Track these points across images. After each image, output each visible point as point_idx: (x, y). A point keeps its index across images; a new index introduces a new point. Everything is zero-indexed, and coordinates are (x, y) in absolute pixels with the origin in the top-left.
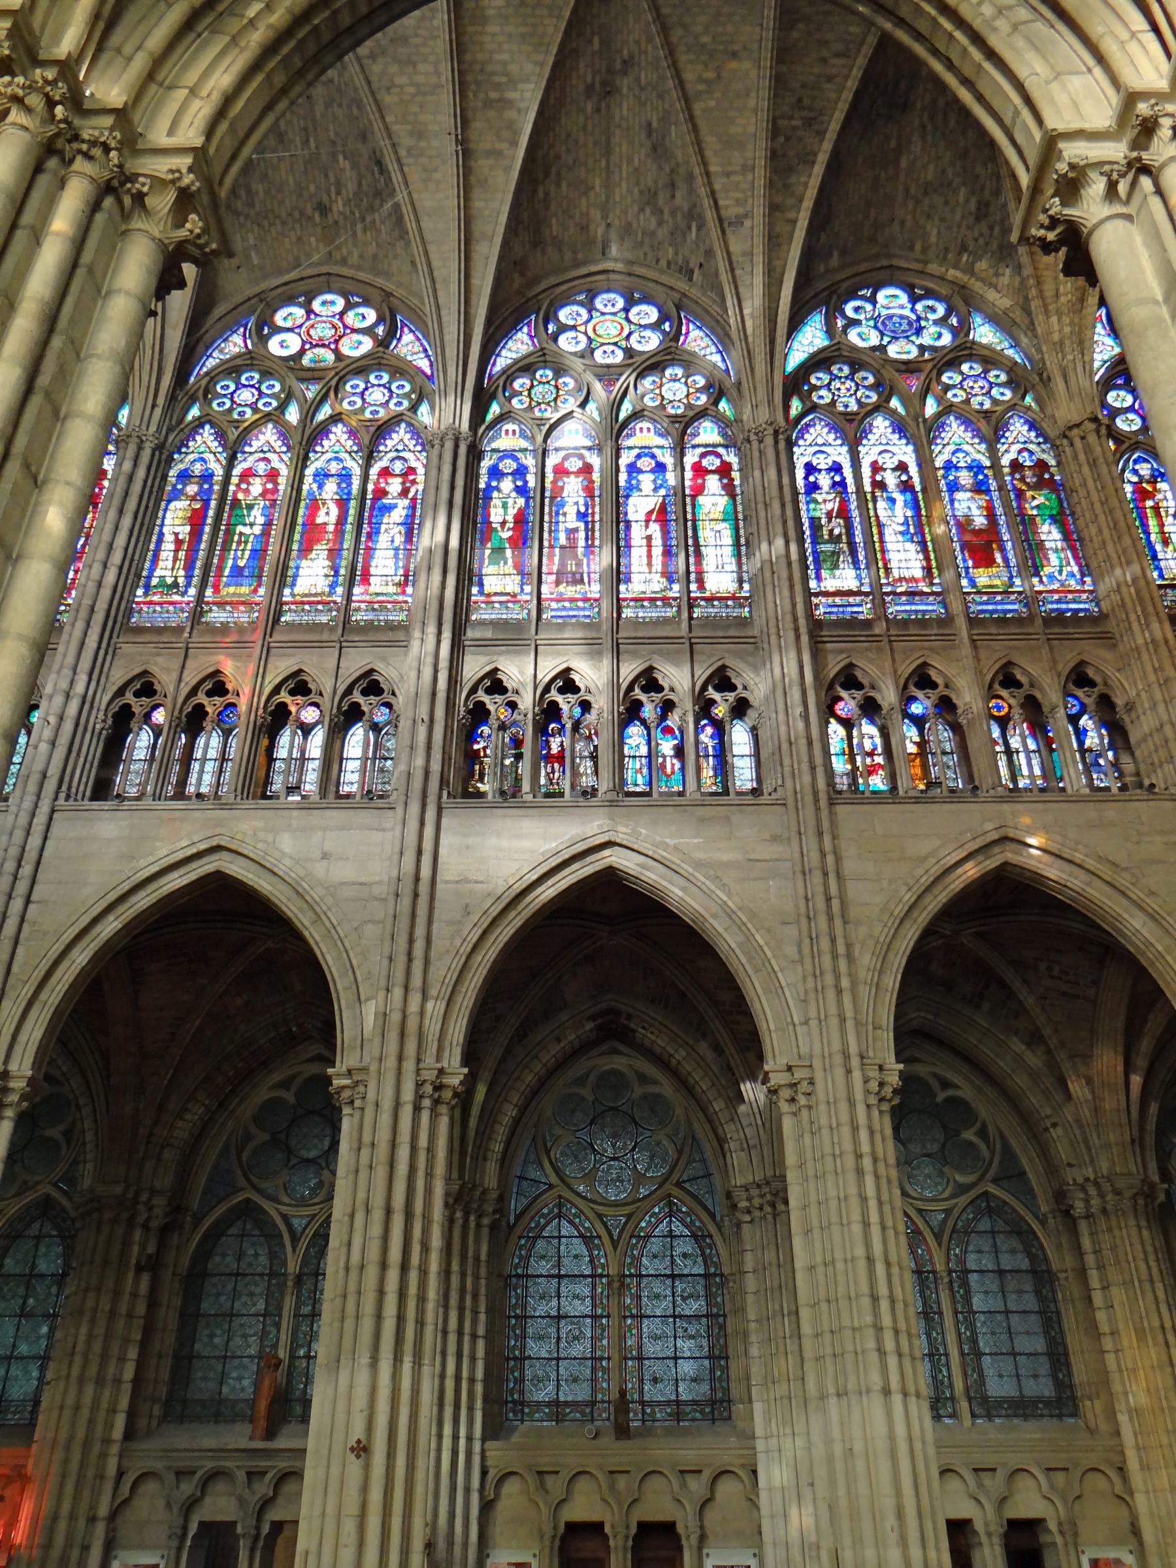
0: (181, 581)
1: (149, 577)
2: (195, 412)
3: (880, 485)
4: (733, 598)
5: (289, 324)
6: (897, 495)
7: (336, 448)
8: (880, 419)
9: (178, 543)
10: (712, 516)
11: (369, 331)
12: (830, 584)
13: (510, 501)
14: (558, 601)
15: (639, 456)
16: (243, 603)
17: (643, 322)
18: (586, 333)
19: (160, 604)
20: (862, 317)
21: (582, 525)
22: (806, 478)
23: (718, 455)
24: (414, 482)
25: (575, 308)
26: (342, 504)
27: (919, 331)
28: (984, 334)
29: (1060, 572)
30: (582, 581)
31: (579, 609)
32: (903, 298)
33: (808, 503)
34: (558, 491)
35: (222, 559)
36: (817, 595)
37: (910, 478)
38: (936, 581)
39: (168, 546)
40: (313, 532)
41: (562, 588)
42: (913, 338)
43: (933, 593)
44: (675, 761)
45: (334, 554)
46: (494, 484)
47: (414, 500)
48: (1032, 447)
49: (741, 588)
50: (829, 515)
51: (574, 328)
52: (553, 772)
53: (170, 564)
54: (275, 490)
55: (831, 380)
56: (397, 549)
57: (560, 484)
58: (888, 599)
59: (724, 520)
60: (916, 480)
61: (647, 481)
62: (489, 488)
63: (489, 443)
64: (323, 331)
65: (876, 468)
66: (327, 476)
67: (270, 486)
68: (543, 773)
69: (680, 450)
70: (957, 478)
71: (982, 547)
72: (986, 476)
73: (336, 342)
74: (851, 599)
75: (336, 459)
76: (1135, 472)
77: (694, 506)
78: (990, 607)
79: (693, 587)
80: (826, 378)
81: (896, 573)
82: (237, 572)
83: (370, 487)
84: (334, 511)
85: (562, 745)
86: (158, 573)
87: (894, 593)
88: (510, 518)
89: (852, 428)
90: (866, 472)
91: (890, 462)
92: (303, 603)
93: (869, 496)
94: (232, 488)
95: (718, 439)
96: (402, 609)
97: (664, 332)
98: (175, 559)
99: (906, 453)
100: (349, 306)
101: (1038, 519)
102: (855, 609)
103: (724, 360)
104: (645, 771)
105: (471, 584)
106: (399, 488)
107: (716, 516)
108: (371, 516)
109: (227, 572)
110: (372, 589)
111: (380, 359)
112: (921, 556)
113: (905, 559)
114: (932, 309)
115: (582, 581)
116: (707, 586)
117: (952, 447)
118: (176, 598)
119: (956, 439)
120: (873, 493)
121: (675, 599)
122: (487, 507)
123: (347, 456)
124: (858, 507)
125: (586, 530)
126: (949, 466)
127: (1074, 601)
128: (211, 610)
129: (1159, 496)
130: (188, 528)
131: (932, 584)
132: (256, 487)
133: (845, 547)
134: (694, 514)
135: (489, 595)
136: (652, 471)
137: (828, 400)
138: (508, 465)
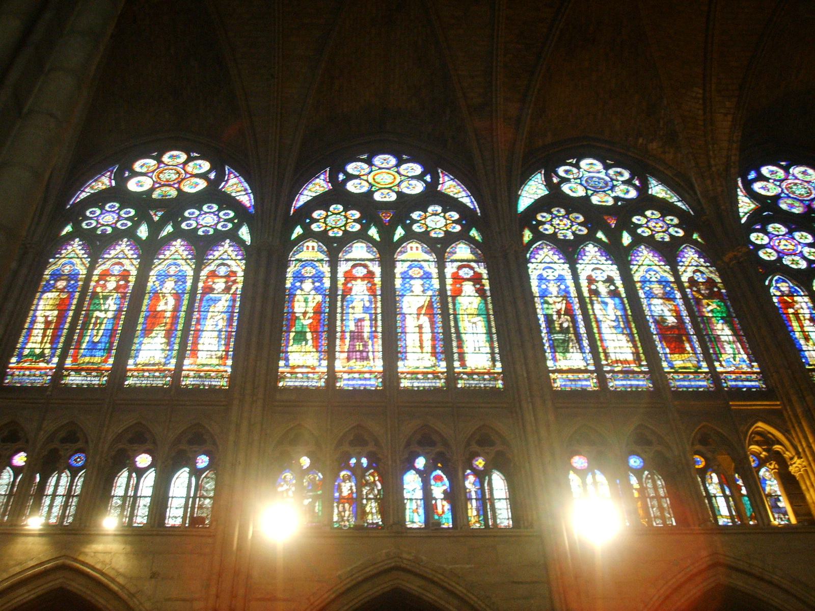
0: (47, 352)
1: (23, 348)
3: (596, 293)
4: (489, 373)
5: (144, 170)
6: (608, 300)
8: (591, 246)
9: (47, 323)
10: (469, 312)
11: (203, 176)
12: (563, 364)
13: (310, 298)
14: (349, 373)
15: (410, 267)
16: (94, 370)
17: (410, 175)
18: (367, 181)
19: (29, 369)
20: (571, 177)
21: (367, 316)
22: (539, 286)
23: (472, 268)
25: (359, 164)
26: (178, 297)
27: (613, 188)
29: (734, 358)
30: (367, 358)
31: (365, 379)
32: (599, 166)
34: (347, 292)
35: (82, 336)
36: (554, 372)
37: (617, 288)
39: (39, 325)
40: (155, 317)
41: (352, 363)
42: (609, 192)
43: (642, 372)
44: (445, 503)
45: (169, 334)
46: (298, 284)
47: (235, 294)
48: (702, 269)
49: (494, 366)
50: (558, 312)
51: (358, 177)
52: (344, 511)
53: (39, 339)
54: (126, 286)
55: (552, 218)
57: (349, 285)
58: (609, 376)
59: (478, 315)
60: (622, 290)
61: (417, 285)
62: (294, 287)
63: (294, 255)
65: (591, 280)
67: (122, 283)
68: (336, 511)
69: (441, 264)
71: (675, 338)
72: (672, 288)
73: (179, 183)
74: (581, 376)
75: (175, 264)
76: (778, 289)
77: (454, 304)
78: (686, 383)
79: (457, 364)
80: (549, 217)
81: (613, 357)
82: (93, 346)
83: (201, 285)
84: (171, 302)
85: (351, 489)
86: (29, 345)
88: (310, 310)
90: (584, 283)
91: (600, 276)
92: (144, 370)
93: (588, 300)
94: (93, 284)
95: (471, 257)
96: (222, 377)
97: (425, 181)
98: (44, 336)
99: (613, 270)
100: (190, 159)
101: (713, 319)
103: (472, 202)
104: (421, 511)
105: (279, 359)
106: (223, 286)
107: (472, 312)
108: (200, 307)
109: (84, 346)
110: (199, 361)
111: (213, 194)
112: (630, 345)
113: (619, 347)
114: (621, 174)
115: (367, 358)
116: (468, 363)
117: (645, 268)
118: (42, 365)
119: (647, 262)
120: (590, 298)
121: (442, 373)
122: (292, 301)
123: (183, 262)
125: (371, 320)
126: (644, 281)
127: (747, 380)
128: (69, 375)
129: (797, 306)
131: (641, 366)
132: (111, 284)
133: (573, 337)
134: (454, 309)
135: (293, 367)
136: (421, 278)
138: (309, 271)
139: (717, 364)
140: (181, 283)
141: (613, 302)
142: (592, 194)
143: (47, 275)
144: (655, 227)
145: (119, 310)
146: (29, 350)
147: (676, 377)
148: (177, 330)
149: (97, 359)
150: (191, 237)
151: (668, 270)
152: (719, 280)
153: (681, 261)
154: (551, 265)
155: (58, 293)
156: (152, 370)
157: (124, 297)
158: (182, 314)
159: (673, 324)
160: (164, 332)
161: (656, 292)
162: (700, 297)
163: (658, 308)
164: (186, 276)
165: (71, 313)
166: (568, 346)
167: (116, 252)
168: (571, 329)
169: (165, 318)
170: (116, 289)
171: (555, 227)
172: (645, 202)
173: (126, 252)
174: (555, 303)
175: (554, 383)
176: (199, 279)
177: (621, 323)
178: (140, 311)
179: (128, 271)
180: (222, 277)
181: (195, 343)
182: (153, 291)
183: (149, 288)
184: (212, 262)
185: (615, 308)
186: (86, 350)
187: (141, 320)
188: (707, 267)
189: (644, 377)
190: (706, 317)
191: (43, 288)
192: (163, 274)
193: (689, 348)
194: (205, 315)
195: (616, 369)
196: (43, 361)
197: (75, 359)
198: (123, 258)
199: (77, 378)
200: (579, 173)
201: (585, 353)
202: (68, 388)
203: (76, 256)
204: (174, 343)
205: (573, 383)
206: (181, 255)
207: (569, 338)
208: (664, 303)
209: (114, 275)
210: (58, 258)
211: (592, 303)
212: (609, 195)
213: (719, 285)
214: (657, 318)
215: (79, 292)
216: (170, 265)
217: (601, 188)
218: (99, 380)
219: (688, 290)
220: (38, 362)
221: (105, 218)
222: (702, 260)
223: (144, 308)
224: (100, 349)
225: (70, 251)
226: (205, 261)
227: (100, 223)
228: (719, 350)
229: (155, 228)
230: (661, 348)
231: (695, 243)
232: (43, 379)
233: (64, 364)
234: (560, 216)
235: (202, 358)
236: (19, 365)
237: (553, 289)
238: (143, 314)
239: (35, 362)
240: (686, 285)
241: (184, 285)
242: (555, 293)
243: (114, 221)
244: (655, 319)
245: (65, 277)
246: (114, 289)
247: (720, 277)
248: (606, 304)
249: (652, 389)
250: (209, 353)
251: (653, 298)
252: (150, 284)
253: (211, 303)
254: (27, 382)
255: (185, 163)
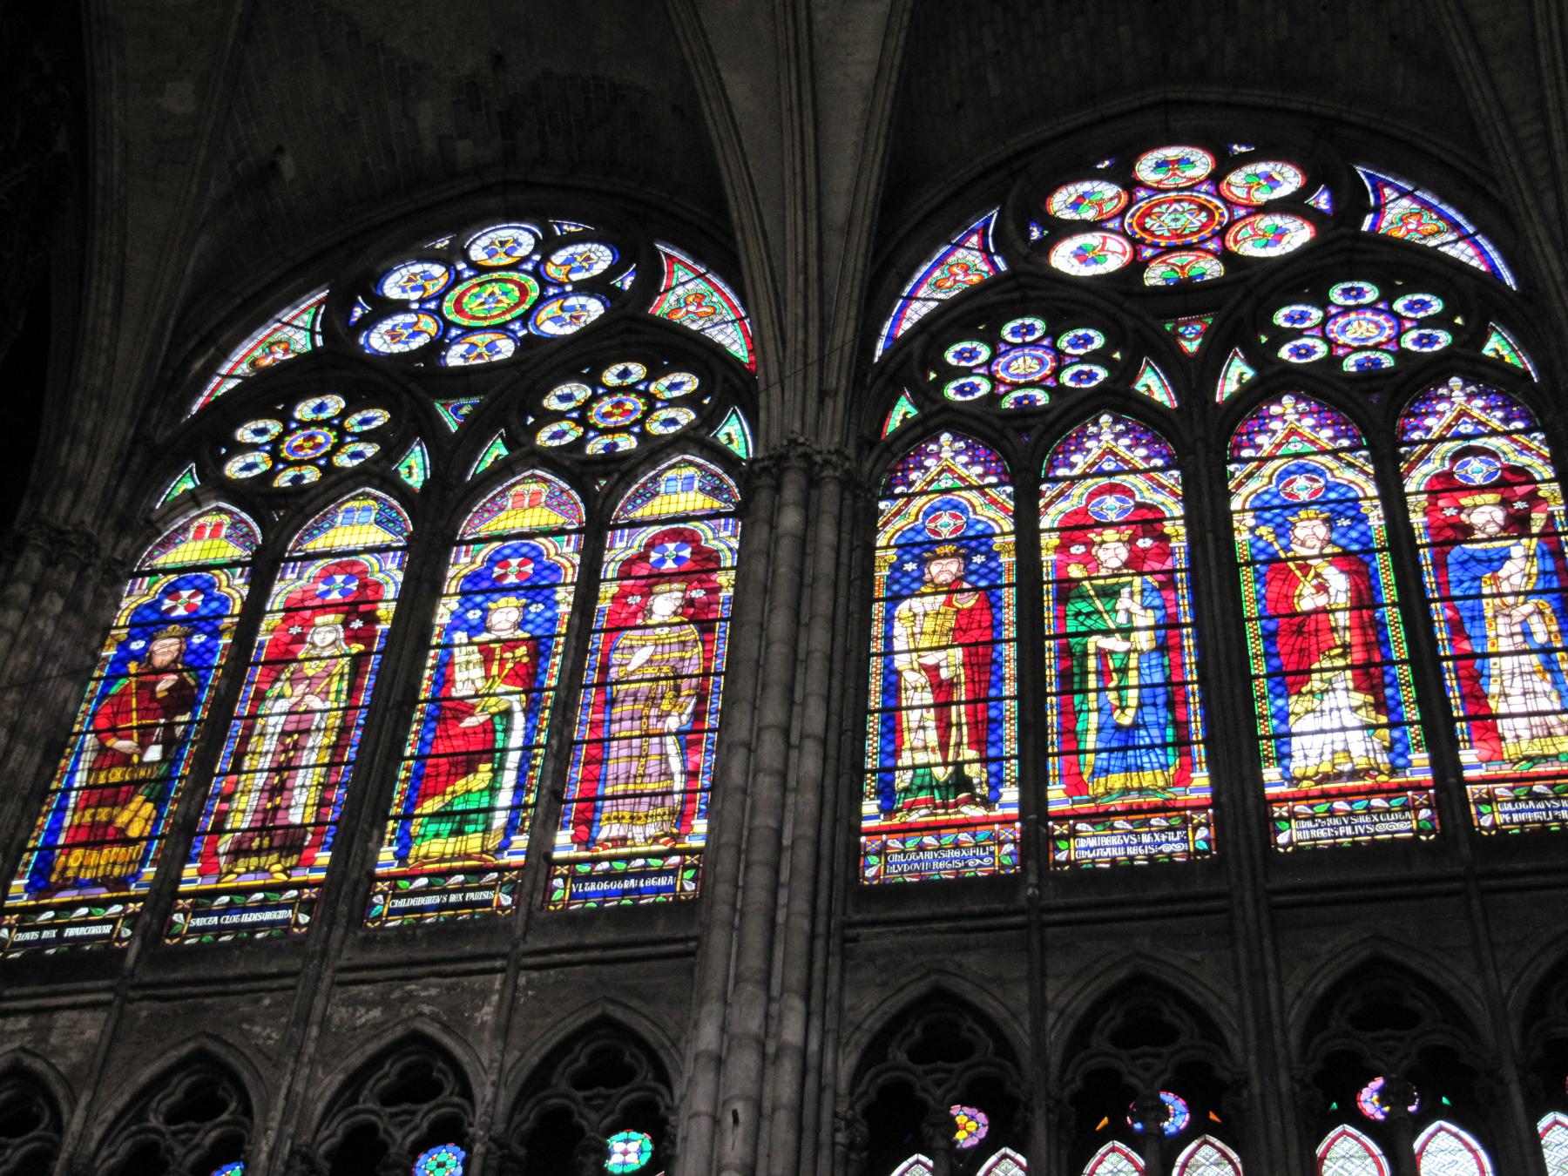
0: (972, 771)
1: (887, 771)
2: (903, 409)
7: (1295, 446)
9: (942, 690)
24: (1534, 499)
26: (1354, 561)
35: (1070, 715)
39: (916, 692)
45: (1371, 677)
53: (932, 737)
56: (1546, 651)
64: (1172, 220)
66: (1295, 507)
67: (1145, 543)
73: (1221, 234)
75: (1302, 470)
82: (1123, 741)
84: (1339, 582)
86: (906, 759)
92: (1326, 796)
94: (1048, 557)
98: (944, 727)
108: (1443, 585)
109: (1091, 742)
123: (1327, 460)
128: (1074, 834)
130: (957, 654)
140: (1348, 522)
143: (888, 547)
145: (1168, 626)
146: (910, 773)
148: (1393, 663)
149: (1147, 779)
150: (1325, 387)
155: (942, 598)
156: (1357, 792)
157: (1168, 583)
158: (1392, 615)
160: (1349, 673)
164: (1357, 499)
165: (1009, 651)
167: (1090, 458)
169: (1334, 630)
170: (1136, 562)
173: (1121, 451)
176: (1405, 503)
178: (1240, 621)
179: (1152, 508)
180: (1481, 489)
181: (1475, 696)
182: (1262, 557)
183: (1243, 553)
184: (1427, 451)
186: (1104, 755)
187: (1255, 646)
191: (888, 589)
192: (1276, 502)
194: (1472, 609)
196: (971, 800)
197: (1076, 786)
198: (1121, 472)
199: (1106, 841)
202: (1082, 876)
203: (959, 484)
204: (1400, 704)
206: (1313, 442)
209: (1111, 525)
210: (902, 495)
215: (1010, 585)
216: (1288, 473)
218: (1185, 840)
220: (956, 805)
221: (1014, 364)
223: (1250, 609)
224: (1152, 747)
225: (934, 471)
226: (1403, 450)
227: (1002, 382)
229: (1194, 377)
232: (992, 854)
233: (1044, 802)
235: (1518, 737)
236: (896, 821)
238: (1253, 630)
239: (945, 806)
241: (1362, 527)
243: (1047, 371)
245: (949, 549)
246: (1126, 565)
250: (1536, 720)
252: (1242, 537)
253: (1477, 570)
254: (942, 868)
255: (1216, 178)
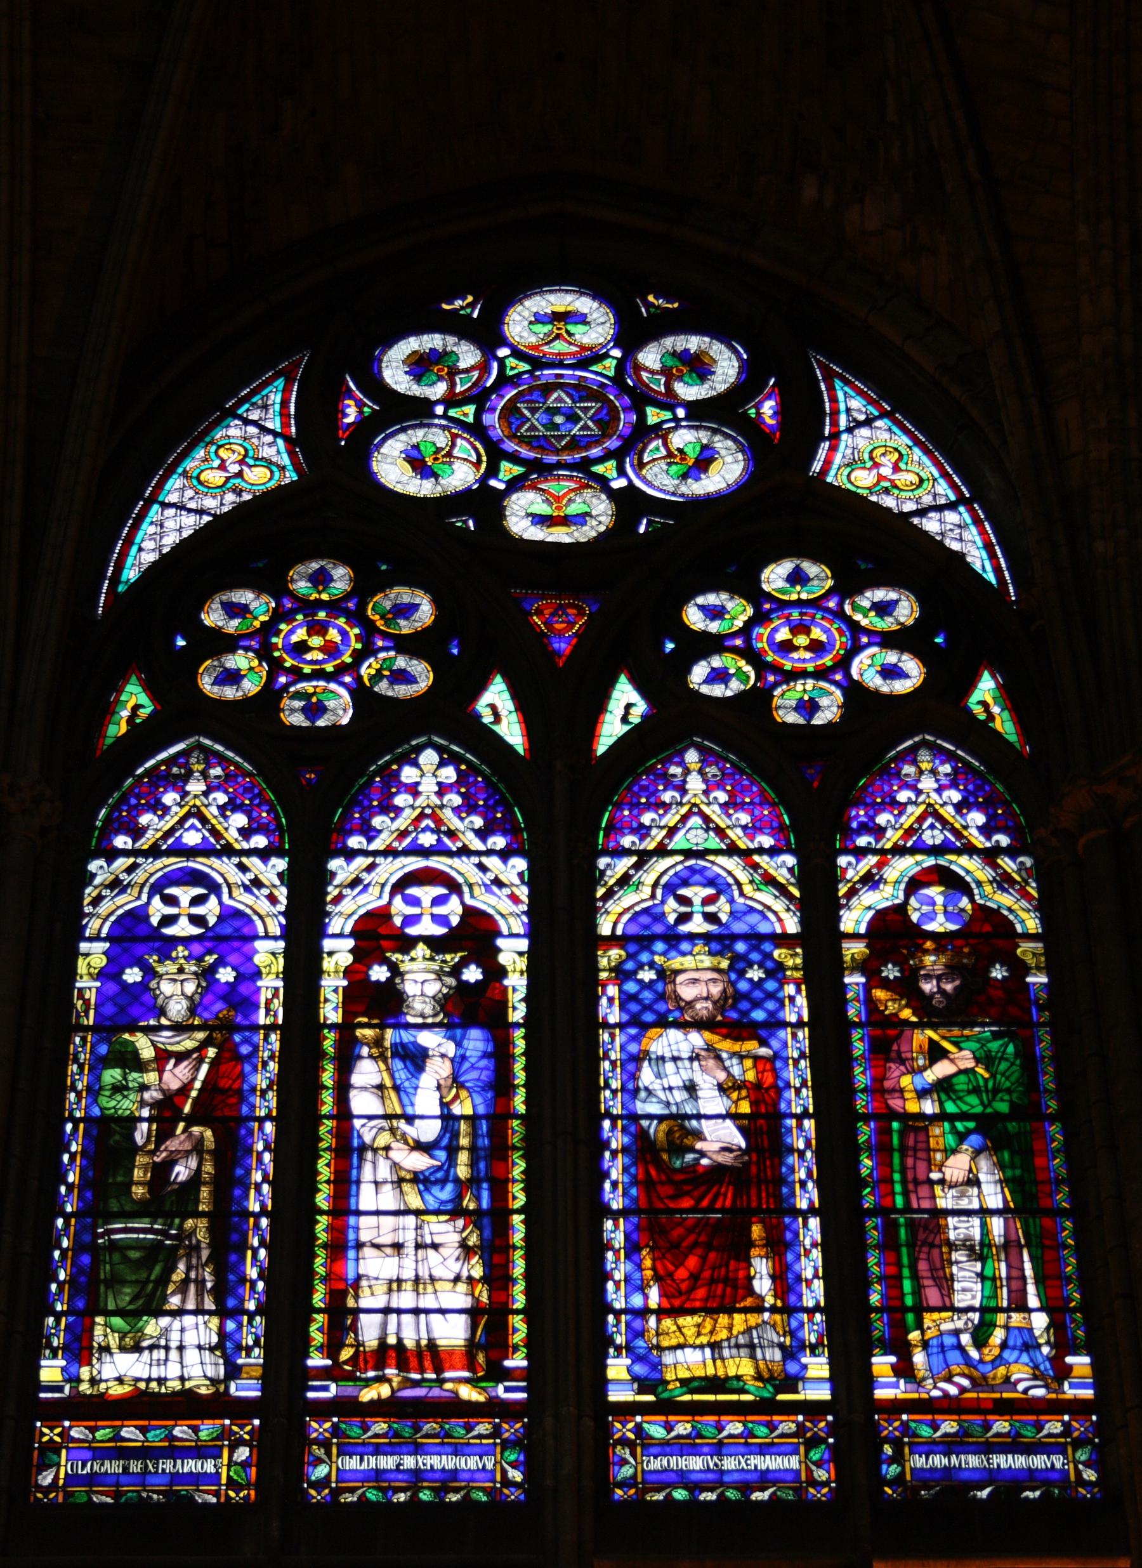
3: (379, 1003)
12: (119, 1370)
22: (109, 974)
28: (875, 457)
29: (980, 1338)
33: (99, 1064)
36: (57, 1411)
38: (517, 1361)
43: (493, 1408)
48: (967, 865)
50: (167, 1111)
55: (279, 615)
60: (516, 983)
70: (666, 975)
71: (708, 1225)
72: (776, 971)
78: (696, 1463)
81: (369, 1330)
87: (347, 1407)
89: (315, 794)
90: (338, 954)
91: (428, 914)
99: (499, 886)
102: (190, 1466)
113: (414, 1273)
114: (699, 366)
119: (693, 836)
120: (345, 1030)
124: (281, 1083)
127: (1014, 1445)
131: (497, 1373)
133: (200, 1228)
137: (251, 686)
139: (882, 1363)
141: (450, 1049)
142: (515, 485)
144: (787, 647)
147: (657, 1431)
151: (782, 876)
152: (1032, 924)
153: (864, 828)
154: (199, 864)
159: (726, 1159)
161: (687, 993)
162: (906, 1014)
163: (684, 1082)
166: (165, 1279)
168: (205, 1192)
171: (276, 667)
172: (788, 507)
174: (163, 1056)
175: (43, 1467)
177: (463, 1157)
185: (456, 1080)
188: (990, 856)
189: (496, 1432)
190: (905, 1117)
193: (763, 1285)
195: (368, 1395)
200: (484, 368)
201: (238, 1312)
205: (135, 1467)
207: (183, 1235)
208: (710, 1048)
211: (346, 1063)
212: (603, 482)
213: (1026, 950)
214: (652, 1127)
217: (575, 444)
219: (855, 980)
222: (977, 818)
228: (918, 1291)
230: (627, 1284)
231: (977, 734)
234: (320, 604)
237: (176, 992)
240: (854, 950)
242: (177, 1009)
244: (643, 1133)
247: (1042, 907)
248: (416, 1058)
249: (513, 1495)
251: (663, 1023)
